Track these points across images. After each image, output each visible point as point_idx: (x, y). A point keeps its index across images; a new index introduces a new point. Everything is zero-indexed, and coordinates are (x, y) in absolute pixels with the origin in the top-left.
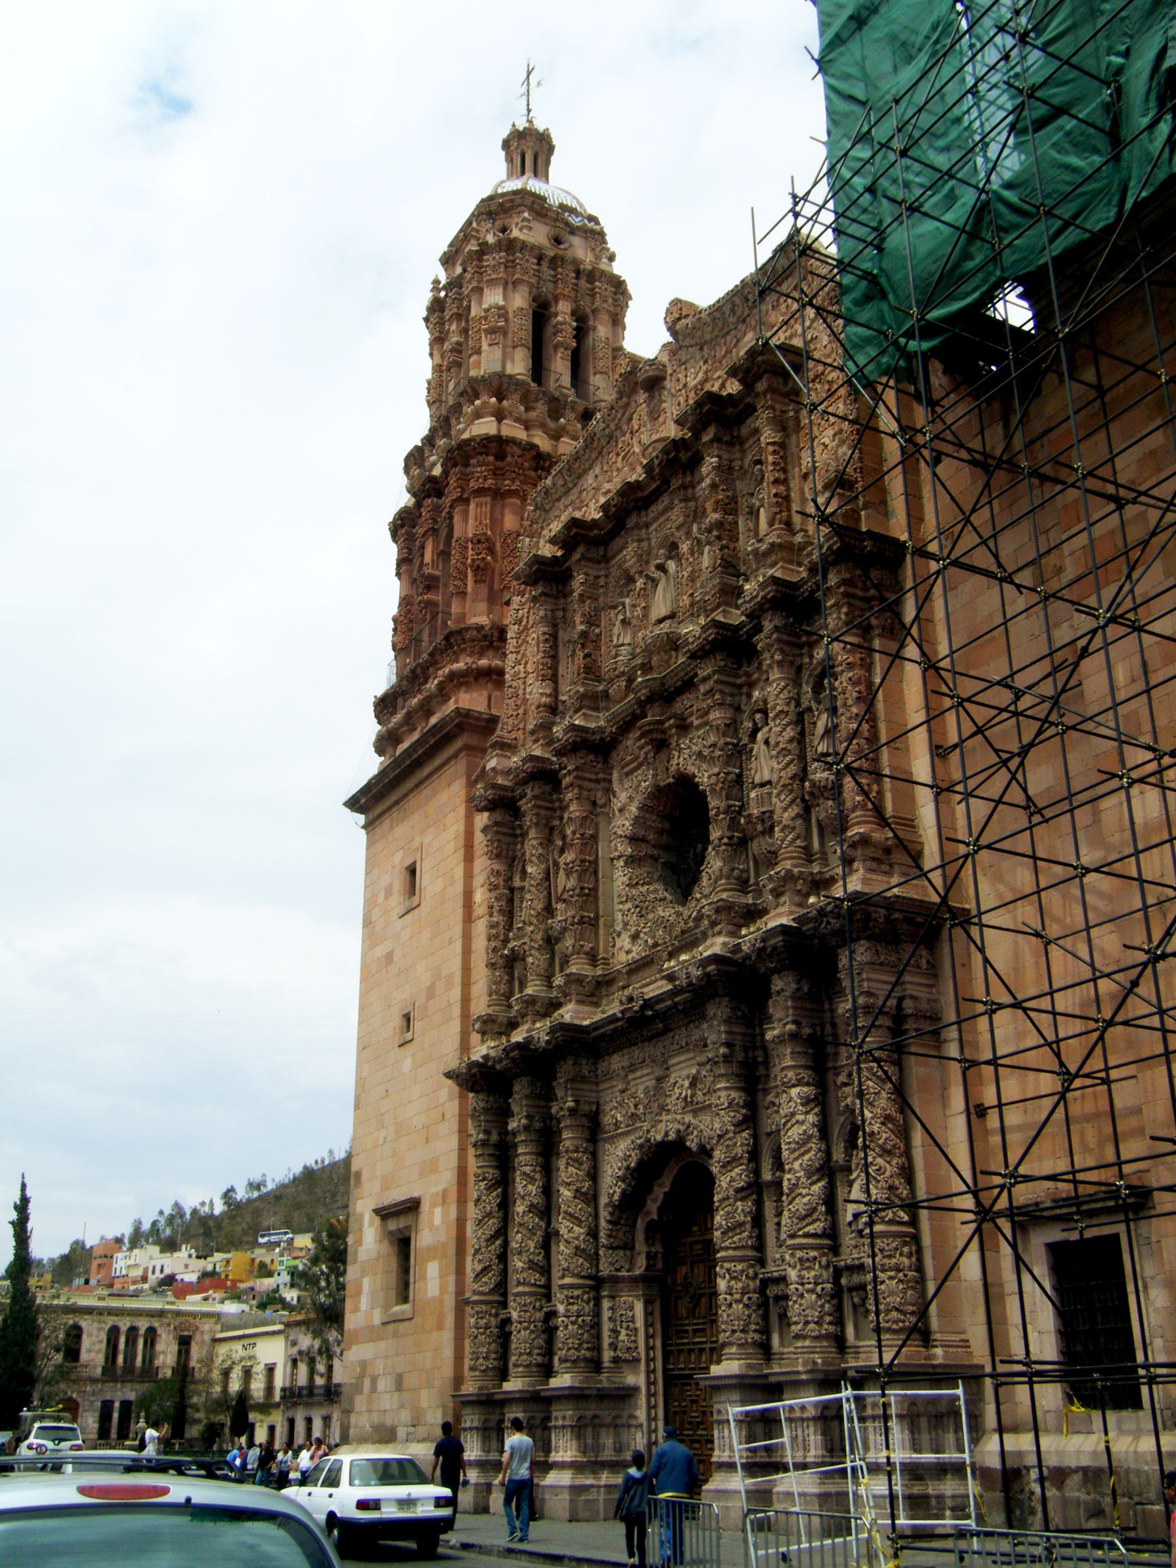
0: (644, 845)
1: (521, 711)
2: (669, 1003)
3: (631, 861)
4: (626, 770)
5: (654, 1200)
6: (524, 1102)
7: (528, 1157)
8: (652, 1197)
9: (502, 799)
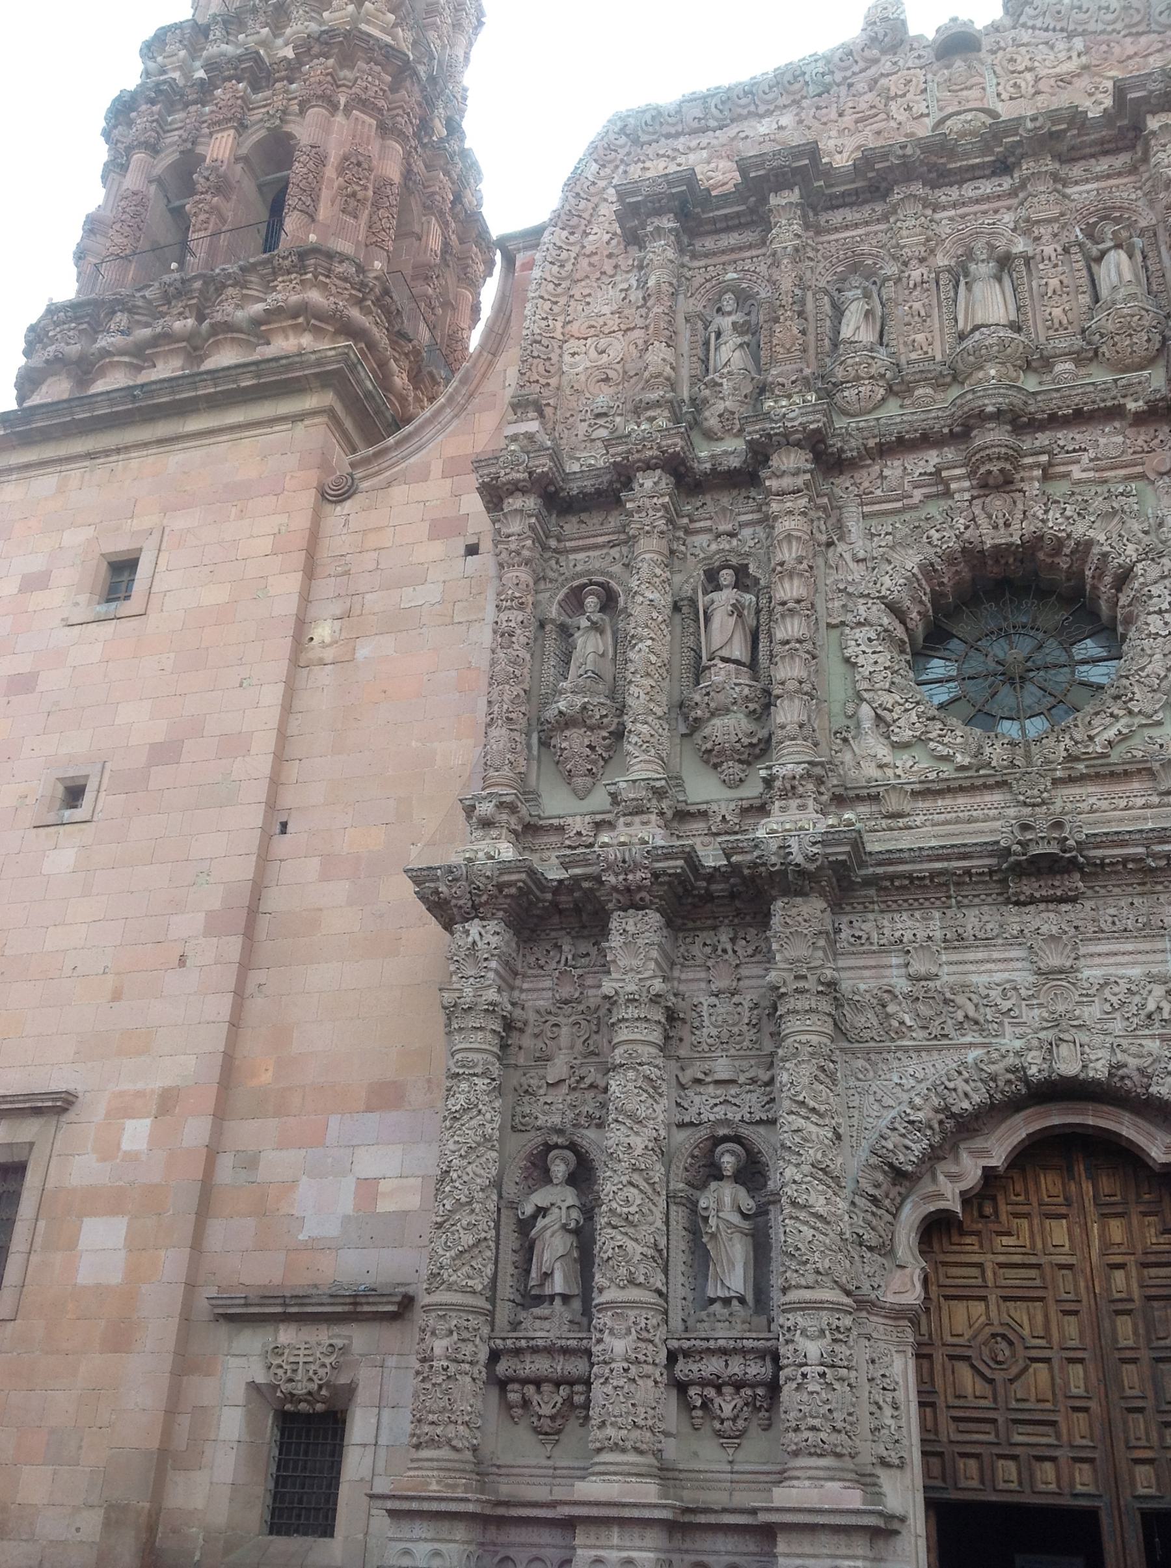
0: (897, 623)
1: (553, 382)
2: (1141, 850)
3: (886, 635)
4: (866, 509)
5: (953, 1177)
6: (655, 954)
7: (654, 1051)
9: (551, 482)
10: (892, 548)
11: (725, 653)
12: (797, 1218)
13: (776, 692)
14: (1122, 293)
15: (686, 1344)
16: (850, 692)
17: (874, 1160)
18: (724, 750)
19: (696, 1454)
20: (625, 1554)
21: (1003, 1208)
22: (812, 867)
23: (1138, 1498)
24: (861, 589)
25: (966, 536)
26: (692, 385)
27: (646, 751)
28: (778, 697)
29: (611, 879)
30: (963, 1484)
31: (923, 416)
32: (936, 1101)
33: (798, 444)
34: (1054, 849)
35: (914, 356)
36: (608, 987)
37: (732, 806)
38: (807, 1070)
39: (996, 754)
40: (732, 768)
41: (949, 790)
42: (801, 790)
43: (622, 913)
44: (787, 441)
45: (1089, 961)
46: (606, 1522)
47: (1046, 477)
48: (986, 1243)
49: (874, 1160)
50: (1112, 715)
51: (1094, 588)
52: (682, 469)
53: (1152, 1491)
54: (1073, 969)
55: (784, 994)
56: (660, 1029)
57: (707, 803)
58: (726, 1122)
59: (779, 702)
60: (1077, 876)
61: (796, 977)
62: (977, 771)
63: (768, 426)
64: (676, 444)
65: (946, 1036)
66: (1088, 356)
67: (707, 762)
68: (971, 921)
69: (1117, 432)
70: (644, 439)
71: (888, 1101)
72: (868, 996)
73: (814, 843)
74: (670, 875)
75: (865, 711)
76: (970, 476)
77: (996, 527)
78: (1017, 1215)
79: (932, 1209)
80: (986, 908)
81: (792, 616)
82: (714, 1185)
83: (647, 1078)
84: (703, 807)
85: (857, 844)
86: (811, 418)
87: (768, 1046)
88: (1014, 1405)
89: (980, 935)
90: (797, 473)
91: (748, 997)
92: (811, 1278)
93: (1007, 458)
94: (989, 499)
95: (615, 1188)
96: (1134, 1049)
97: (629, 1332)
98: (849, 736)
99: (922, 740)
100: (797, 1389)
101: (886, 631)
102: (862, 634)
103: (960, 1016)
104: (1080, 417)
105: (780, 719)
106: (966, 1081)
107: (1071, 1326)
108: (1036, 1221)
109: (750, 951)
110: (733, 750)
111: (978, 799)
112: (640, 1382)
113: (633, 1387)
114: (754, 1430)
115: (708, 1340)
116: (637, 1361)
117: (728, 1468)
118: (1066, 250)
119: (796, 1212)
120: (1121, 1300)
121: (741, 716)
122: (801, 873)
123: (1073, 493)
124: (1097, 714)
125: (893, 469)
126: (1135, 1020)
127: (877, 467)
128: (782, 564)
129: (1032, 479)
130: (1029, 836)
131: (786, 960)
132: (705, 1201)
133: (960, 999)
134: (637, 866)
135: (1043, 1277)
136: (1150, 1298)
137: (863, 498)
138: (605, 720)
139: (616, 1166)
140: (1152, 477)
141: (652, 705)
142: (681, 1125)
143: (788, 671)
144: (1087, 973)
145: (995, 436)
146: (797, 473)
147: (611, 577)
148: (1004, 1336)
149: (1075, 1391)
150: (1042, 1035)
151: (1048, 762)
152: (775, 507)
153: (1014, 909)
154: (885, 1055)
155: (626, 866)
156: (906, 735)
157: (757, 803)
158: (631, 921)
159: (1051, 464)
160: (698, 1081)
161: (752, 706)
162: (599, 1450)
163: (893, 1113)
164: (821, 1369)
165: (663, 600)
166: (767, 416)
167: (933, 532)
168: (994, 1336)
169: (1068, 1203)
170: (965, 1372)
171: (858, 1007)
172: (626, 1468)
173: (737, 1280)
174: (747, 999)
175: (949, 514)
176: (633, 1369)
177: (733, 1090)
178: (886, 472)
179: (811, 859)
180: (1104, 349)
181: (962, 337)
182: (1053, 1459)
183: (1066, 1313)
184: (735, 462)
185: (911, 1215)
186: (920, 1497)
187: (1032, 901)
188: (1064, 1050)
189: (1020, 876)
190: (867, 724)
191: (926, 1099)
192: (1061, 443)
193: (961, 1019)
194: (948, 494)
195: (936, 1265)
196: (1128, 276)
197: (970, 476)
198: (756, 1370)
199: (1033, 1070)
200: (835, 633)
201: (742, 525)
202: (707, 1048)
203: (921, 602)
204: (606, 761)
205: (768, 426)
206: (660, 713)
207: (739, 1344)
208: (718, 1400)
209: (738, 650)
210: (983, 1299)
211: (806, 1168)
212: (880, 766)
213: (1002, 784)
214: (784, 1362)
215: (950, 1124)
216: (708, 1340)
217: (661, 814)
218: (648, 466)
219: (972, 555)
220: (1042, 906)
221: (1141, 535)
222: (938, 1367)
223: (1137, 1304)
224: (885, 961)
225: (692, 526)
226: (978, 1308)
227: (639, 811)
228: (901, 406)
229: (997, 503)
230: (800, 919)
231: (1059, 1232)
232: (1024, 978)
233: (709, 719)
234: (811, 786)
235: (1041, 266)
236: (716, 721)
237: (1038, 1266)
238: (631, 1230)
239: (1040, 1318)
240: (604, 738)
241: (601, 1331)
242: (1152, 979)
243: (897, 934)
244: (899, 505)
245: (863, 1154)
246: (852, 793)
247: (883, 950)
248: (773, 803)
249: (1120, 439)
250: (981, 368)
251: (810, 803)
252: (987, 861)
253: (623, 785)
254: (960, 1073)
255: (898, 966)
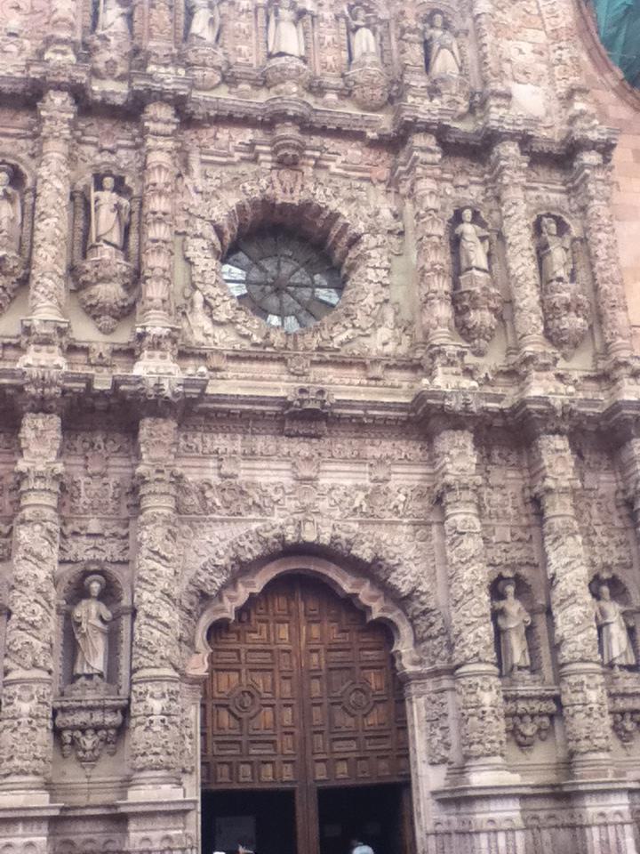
2: (361, 412)
4: (204, 157)
5: (232, 599)
7: (52, 512)
8: (233, 594)
10: (220, 188)
11: (107, 238)
12: (149, 625)
13: (148, 273)
14: (369, 59)
15: (65, 704)
16: (187, 281)
17: (192, 588)
18: (104, 307)
19: (64, 774)
20: (27, 840)
21: (253, 617)
22: (176, 400)
23: (316, 781)
24: (199, 212)
25: (268, 192)
26: (84, 33)
27: (51, 299)
28: (148, 278)
29: (31, 390)
30: (220, 780)
31: (247, 105)
32: (232, 554)
33: (168, 102)
34: (317, 406)
35: (240, 60)
36: (22, 465)
37: (108, 347)
38: (160, 532)
39: (277, 338)
40: (107, 320)
41: (250, 358)
42: (163, 346)
43: (34, 415)
44: (161, 97)
45: (325, 475)
46: (14, 821)
47: (316, 166)
48: (242, 637)
49: (192, 588)
50: (344, 326)
51: (334, 242)
52: (82, 96)
53: (324, 777)
54: (316, 479)
55: (148, 482)
56: (55, 497)
57: (90, 342)
58: (98, 562)
59: (148, 281)
60: (324, 423)
61: (159, 471)
62: (265, 348)
63: (149, 83)
64: (81, 77)
65: (240, 514)
66: (346, 94)
67: (88, 313)
68: (262, 443)
69: (358, 148)
70: (60, 67)
71: (202, 552)
72: (193, 485)
73: (179, 385)
74: (74, 393)
75: (198, 297)
76: (274, 153)
77: (285, 191)
78: (261, 621)
79: (218, 617)
80: (269, 436)
81: (160, 223)
82: (84, 602)
83: (49, 531)
84: (86, 345)
85: (204, 388)
86: (183, 87)
87: (125, 513)
88: (251, 732)
89: (264, 453)
90: (168, 122)
91: (113, 480)
92: (158, 662)
93: (294, 147)
94: (282, 171)
95: (24, 604)
96: (345, 528)
97: (32, 697)
98: (187, 312)
99: (232, 322)
100: (145, 730)
101: (213, 244)
102: (199, 243)
103: (250, 502)
104: (339, 133)
105: (149, 294)
106: (251, 542)
107: (287, 687)
108: (271, 625)
109: (116, 448)
110: (111, 309)
111: (265, 366)
112: (38, 729)
113: (34, 733)
114: (105, 757)
115: (80, 701)
116: (37, 717)
117: (86, 780)
118: (337, 18)
119: (148, 621)
120: (315, 671)
121: (118, 285)
122: (167, 401)
123: (331, 181)
124: (336, 324)
125: (224, 134)
126: (347, 511)
127: (212, 131)
128: (155, 185)
129: (308, 165)
130: (305, 396)
131: (150, 459)
132: (79, 612)
133: (251, 492)
134: (53, 384)
135: (272, 657)
136: (331, 669)
137: (203, 149)
138: (17, 270)
139: (24, 589)
140: (375, 181)
141: (56, 266)
142: (62, 562)
143: (155, 262)
144: (322, 482)
145: (289, 131)
146: (168, 122)
147: (21, 162)
148: (249, 692)
149: (286, 723)
150: (295, 516)
151: (306, 349)
152: (150, 142)
153: (286, 439)
154: (202, 523)
155: (43, 382)
156: (223, 317)
157: (125, 348)
158: (40, 421)
159: (320, 159)
160: (75, 533)
161: (127, 280)
162: (7, 775)
163: (205, 560)
164: (163, 717)
165: (66, 190)
166: (150, 77)
167: (246, 184)
168: (243, 692)
169: (290, 614)
170: (224, 715)
171: (187, 492)
172: (29, 786)
173: (98, 664)
174: (112, 480)
175: (257, 176)
176: (35, 723)
177: (100, 540)
178: (219, 135)
179: (175, 394)
180: (356, 92)
181: (270, 56)
182: (272, 762)
183: (285, 678)
184: (119, 101)
185: (205, 621)
186: (199, 789)
187: (297, 435)
188: (308, 526)
189: (293, 420)
190: (199, 305)
191: (226, 551)
192: (326, 146)
193: (251, 503)
194: (255, 160)
195: (217, 650)
196: (373, 49)
197: (274, 153)
198: (112, 719)
199: (289, 538)
200: (179, 239)
201: (120, 147)
202: (82, 511)
203: (233, 228)
204: (12, 299)
205: (149, 83)
206: (61, 274)
207: (102, 703)
208: (83, 739)
209: (116, 238)
210: (238, 671)
211: (158, 594)
212: (206, 335)
213: (282, 360)
214: (133, 713)
215: (237, 568)
216: (80, 701)
217: (61, 347)
218: (59, 87)
219: (267, 205)
220: (301, 439)
221: (366, 217)
222: (209, 713)
223: (323, 673)
224: (205, 463)
225: (83, 138)
226: (235, 676)
227: (46, 342)
228: (230, 92)
229: (287, 175)
230: (161, 433)
231: (284, 632)
232: (286, 479)
233: (95, 284)
234: (169, 344)
235: (321, 24)
236: (100, 286)
237: (270, 651)
238: (34, 632)
239: (270, 681)
240: (13, 283)
241: (10, 698)
242: (358, 488)
243: (215, 447)
244: (224, 160)
245: (185, 584)
246: (189, 351)
247: (204, 457)
248: (142, 351)
249: (359, 153)
250: (283, 82)
251: (169, 356)
252: (276, 408)
253: (36, 323)
254: (247, 537)
255: (214, 468)
